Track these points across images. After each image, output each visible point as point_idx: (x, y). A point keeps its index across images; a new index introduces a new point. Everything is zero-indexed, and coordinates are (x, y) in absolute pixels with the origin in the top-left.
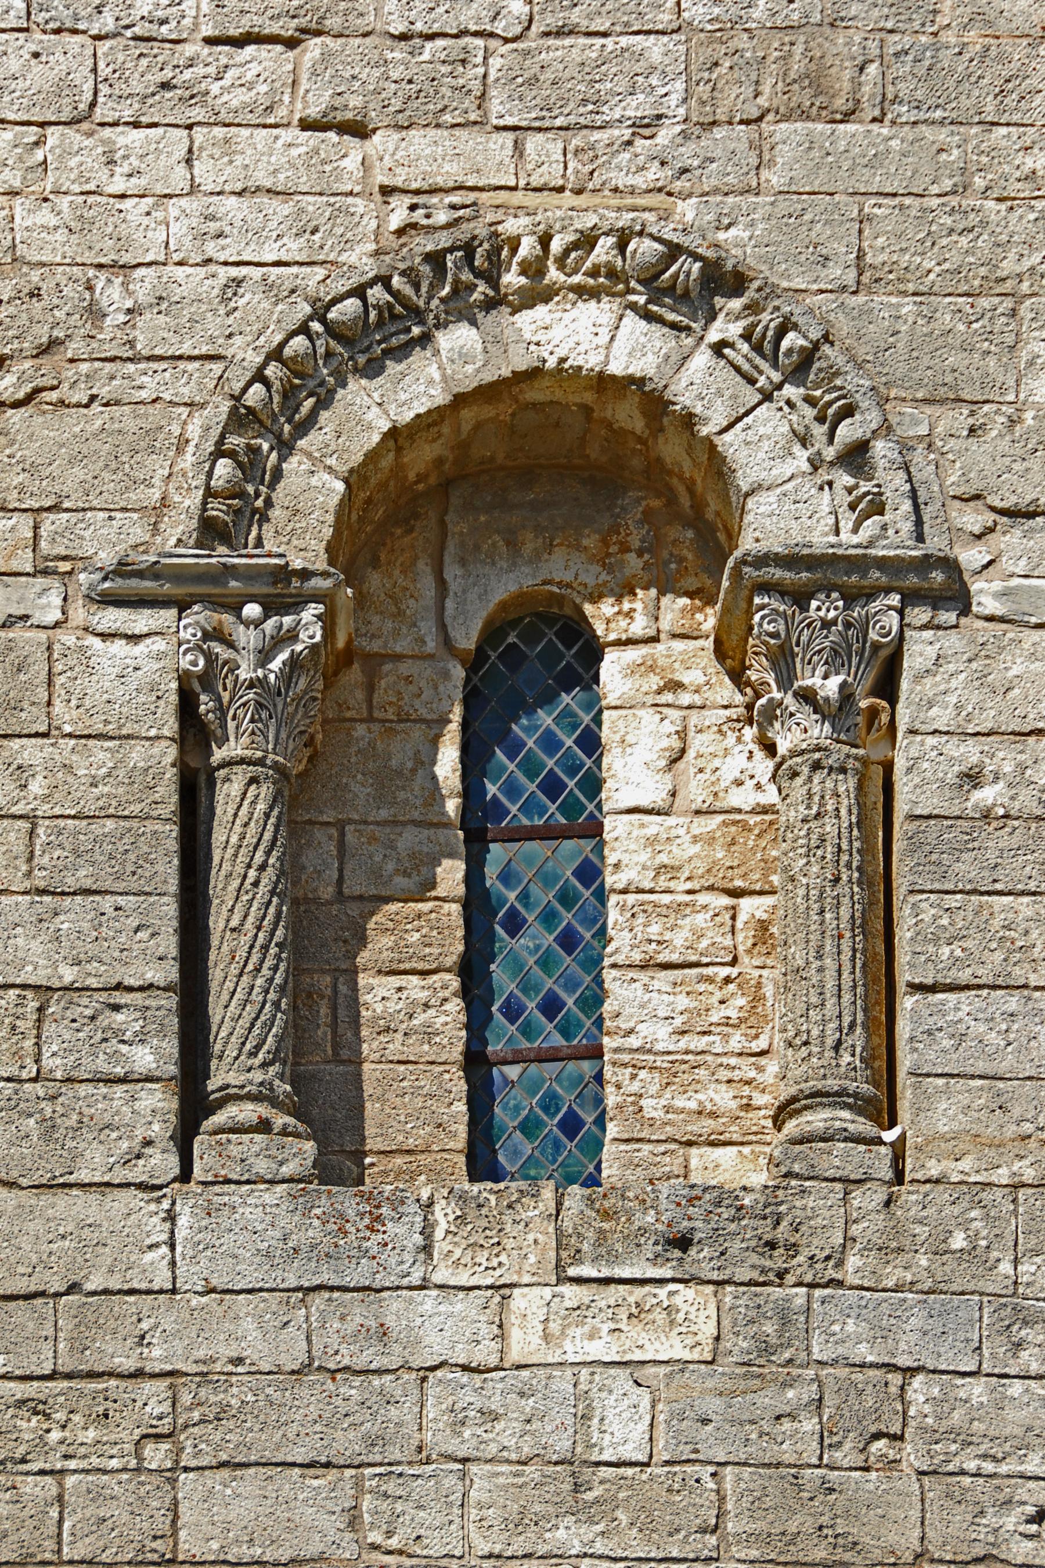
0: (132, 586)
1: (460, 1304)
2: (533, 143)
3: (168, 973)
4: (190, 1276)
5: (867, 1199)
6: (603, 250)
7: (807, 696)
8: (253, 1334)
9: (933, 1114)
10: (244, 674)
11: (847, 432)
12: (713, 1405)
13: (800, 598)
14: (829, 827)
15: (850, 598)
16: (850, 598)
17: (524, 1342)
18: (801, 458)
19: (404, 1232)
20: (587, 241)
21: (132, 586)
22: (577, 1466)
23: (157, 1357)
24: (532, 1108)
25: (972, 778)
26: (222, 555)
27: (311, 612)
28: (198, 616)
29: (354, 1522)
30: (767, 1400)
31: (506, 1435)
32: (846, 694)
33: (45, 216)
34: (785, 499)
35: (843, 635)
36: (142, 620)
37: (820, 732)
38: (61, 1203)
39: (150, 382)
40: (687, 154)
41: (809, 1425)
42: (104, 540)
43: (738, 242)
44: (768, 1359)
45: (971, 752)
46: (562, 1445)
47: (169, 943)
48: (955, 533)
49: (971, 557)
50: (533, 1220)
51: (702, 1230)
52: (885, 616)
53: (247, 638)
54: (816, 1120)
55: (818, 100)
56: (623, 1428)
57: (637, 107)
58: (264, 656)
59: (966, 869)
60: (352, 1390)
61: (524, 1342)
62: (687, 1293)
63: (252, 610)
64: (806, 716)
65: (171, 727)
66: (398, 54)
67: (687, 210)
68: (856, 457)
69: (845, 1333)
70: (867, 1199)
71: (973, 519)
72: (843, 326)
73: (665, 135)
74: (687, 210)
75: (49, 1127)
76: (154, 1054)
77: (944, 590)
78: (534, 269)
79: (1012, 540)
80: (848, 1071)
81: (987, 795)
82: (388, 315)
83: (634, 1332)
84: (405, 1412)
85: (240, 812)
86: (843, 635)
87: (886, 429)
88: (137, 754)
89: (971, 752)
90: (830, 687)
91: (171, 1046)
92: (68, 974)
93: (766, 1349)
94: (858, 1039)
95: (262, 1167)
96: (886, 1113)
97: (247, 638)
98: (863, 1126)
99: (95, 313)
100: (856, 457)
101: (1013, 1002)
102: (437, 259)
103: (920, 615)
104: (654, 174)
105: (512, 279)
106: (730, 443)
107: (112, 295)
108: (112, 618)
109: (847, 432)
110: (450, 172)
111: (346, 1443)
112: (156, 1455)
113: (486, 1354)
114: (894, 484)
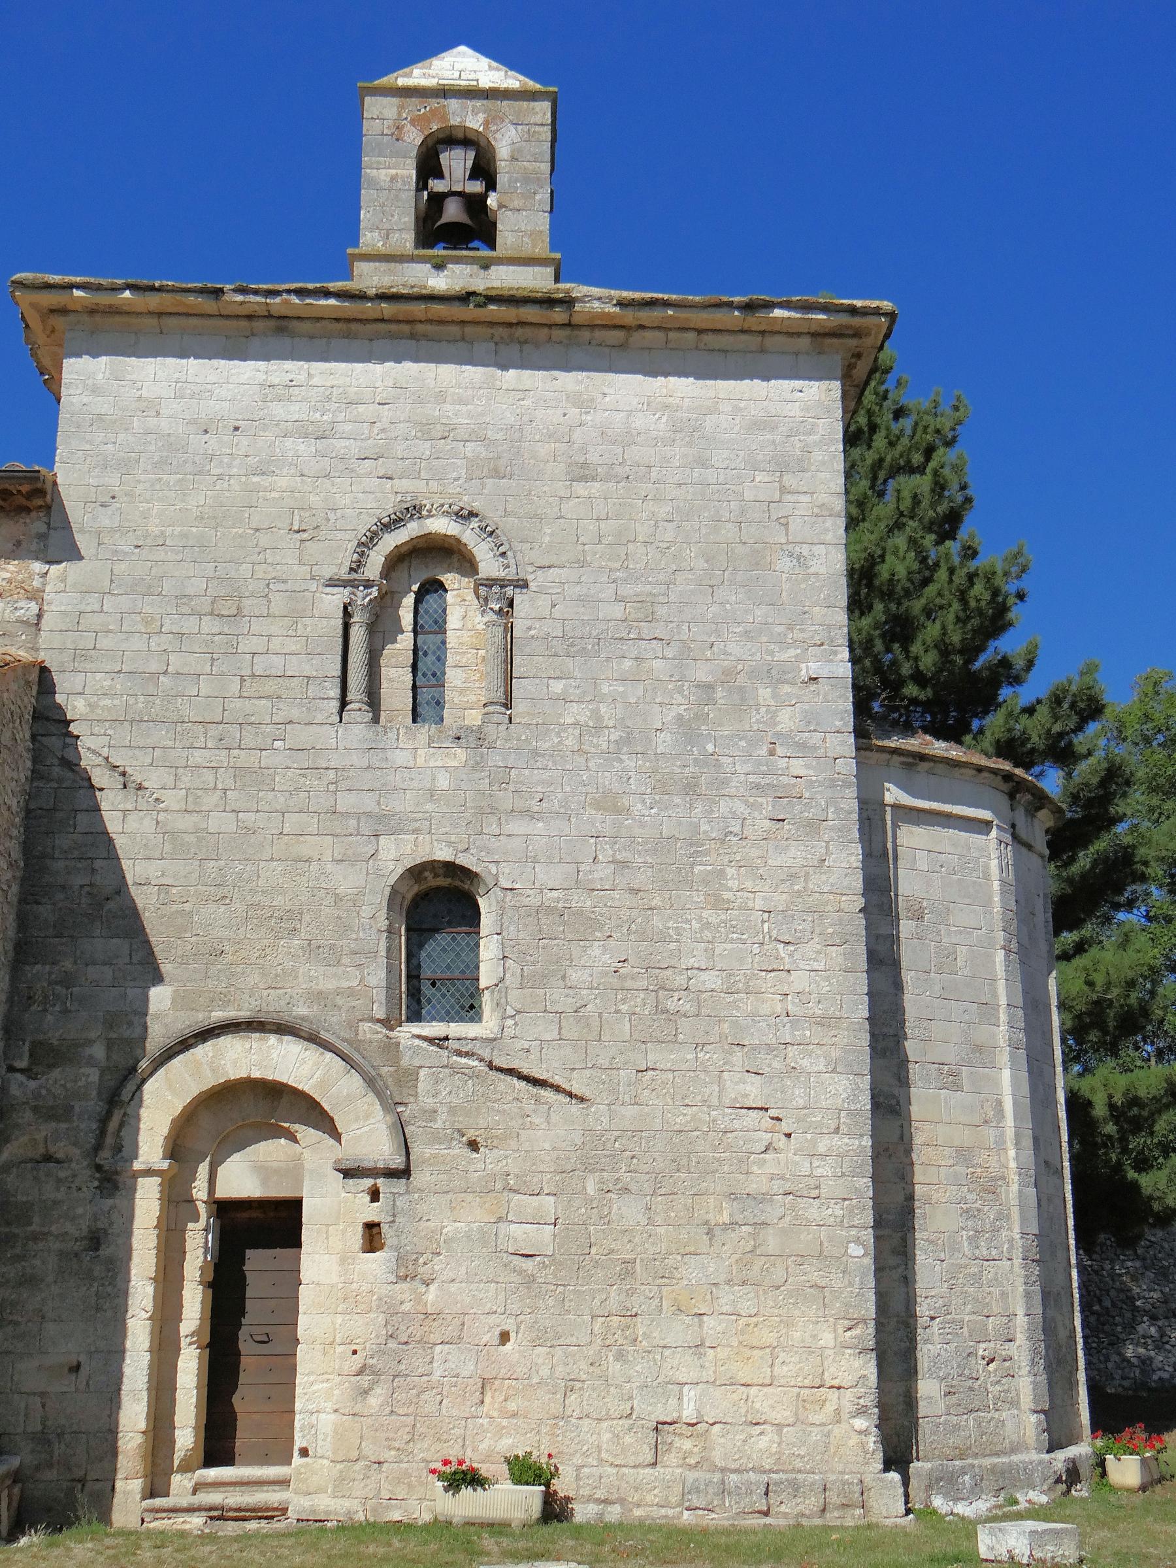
0: (333, 583)
1: (405, 753)
2: (431, 483)
3: (339, 673)
4: (341, 746)
5: (502, 728)
6: (446, 507)
7: (491, 609)
8: (356, 759)
9: (519, 707)
10: (359, 603)
11: (502, 549)
12: (464, 777)
13: (491, 587)
14: (496, 639)
15: (502, 587)
16: (502, 587)
17: (420, 761)
18: (492, 554)
19: (392, 735)
20: (442, 505)
21: (333, 583)
22: (432, 792)
23: (332, 764)
24: (426, 704)
25: (530, 628)
26: (354, 576)
27: (376, 588)
28: (349, 589)
29: (379, 803)
30: (477, 775)
31: (415, 784)
32: (501, 609)
33: (317, 498)
34: (489, 566)
35: (502, 595)
36: (336, 590)
37: (495, 617)
38: (311, 727)
39: (339, 535)
40: (466, 486)
41: (487, 781)
42: (328, 572)
43: (477, 506)
44: (478, 766)
45: (529, 623)
46: (428, 786)
47: (339, 666)
48: (526, 572)
49: (530, 577)
50: (424, 731)
51: (463, 735)
52: (509, 591)
53: (360, 594)
54: (491, 708)
55: (497, 474)
56: (443, 782)
57: (455, 475)
58: (364, 598)
59: (527, 650)
60: (379, 773)
61: (420, 761)
62: (459, 750)
63: (361, 588)
64: (491, 613)
65: (341, 615)
66: (400, 462)
67: (466, 498)
68: (503, 554)
69: (495, 759)
70: (502, 728)
71: (530, 569)
72: (501, 525)
73: (460, 482)
74: (466, 498)
75: (309, 709)
76: (335, 692)
77: (523, 584)
78: (429, 511)
79: (540, 573)
80: (499, 696)
81: (532, 632)
82: (395, 521)
83: (446, 759)
84: (392, 778)
85: (358, 634)
86: (502, 595)
87: (511, 548)
88: (333, 622)
89: (529, 623)
90: (497, 607)
91: (338, 691)
92: (314, 674)
93: (478, 763)
94: (502, 689)
95: (359, 720)
96: (508, 704)
97: (360, 594)
98: (503, 709)
99: (328, 520)
100: (503, 554)
101: (538, 681)
102: (407, 509)
103: (518, 590)
104: (458, 490)
105: (424, 513)
106: (475, 551)
107: (331, 516)
108: (329, 589)
109: (502, 549)
110: (411, 489)
111: (377, 785)
112: (332, 788)
113: (411, 764)
114: (512, 561)
